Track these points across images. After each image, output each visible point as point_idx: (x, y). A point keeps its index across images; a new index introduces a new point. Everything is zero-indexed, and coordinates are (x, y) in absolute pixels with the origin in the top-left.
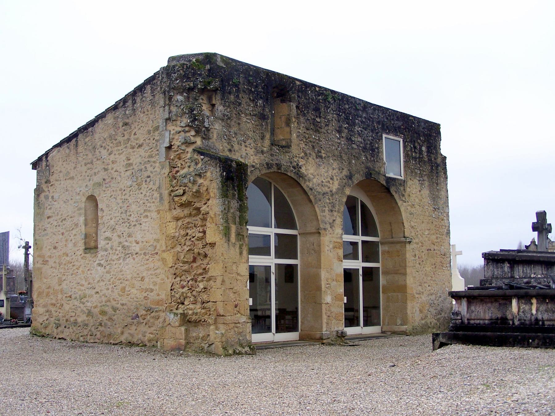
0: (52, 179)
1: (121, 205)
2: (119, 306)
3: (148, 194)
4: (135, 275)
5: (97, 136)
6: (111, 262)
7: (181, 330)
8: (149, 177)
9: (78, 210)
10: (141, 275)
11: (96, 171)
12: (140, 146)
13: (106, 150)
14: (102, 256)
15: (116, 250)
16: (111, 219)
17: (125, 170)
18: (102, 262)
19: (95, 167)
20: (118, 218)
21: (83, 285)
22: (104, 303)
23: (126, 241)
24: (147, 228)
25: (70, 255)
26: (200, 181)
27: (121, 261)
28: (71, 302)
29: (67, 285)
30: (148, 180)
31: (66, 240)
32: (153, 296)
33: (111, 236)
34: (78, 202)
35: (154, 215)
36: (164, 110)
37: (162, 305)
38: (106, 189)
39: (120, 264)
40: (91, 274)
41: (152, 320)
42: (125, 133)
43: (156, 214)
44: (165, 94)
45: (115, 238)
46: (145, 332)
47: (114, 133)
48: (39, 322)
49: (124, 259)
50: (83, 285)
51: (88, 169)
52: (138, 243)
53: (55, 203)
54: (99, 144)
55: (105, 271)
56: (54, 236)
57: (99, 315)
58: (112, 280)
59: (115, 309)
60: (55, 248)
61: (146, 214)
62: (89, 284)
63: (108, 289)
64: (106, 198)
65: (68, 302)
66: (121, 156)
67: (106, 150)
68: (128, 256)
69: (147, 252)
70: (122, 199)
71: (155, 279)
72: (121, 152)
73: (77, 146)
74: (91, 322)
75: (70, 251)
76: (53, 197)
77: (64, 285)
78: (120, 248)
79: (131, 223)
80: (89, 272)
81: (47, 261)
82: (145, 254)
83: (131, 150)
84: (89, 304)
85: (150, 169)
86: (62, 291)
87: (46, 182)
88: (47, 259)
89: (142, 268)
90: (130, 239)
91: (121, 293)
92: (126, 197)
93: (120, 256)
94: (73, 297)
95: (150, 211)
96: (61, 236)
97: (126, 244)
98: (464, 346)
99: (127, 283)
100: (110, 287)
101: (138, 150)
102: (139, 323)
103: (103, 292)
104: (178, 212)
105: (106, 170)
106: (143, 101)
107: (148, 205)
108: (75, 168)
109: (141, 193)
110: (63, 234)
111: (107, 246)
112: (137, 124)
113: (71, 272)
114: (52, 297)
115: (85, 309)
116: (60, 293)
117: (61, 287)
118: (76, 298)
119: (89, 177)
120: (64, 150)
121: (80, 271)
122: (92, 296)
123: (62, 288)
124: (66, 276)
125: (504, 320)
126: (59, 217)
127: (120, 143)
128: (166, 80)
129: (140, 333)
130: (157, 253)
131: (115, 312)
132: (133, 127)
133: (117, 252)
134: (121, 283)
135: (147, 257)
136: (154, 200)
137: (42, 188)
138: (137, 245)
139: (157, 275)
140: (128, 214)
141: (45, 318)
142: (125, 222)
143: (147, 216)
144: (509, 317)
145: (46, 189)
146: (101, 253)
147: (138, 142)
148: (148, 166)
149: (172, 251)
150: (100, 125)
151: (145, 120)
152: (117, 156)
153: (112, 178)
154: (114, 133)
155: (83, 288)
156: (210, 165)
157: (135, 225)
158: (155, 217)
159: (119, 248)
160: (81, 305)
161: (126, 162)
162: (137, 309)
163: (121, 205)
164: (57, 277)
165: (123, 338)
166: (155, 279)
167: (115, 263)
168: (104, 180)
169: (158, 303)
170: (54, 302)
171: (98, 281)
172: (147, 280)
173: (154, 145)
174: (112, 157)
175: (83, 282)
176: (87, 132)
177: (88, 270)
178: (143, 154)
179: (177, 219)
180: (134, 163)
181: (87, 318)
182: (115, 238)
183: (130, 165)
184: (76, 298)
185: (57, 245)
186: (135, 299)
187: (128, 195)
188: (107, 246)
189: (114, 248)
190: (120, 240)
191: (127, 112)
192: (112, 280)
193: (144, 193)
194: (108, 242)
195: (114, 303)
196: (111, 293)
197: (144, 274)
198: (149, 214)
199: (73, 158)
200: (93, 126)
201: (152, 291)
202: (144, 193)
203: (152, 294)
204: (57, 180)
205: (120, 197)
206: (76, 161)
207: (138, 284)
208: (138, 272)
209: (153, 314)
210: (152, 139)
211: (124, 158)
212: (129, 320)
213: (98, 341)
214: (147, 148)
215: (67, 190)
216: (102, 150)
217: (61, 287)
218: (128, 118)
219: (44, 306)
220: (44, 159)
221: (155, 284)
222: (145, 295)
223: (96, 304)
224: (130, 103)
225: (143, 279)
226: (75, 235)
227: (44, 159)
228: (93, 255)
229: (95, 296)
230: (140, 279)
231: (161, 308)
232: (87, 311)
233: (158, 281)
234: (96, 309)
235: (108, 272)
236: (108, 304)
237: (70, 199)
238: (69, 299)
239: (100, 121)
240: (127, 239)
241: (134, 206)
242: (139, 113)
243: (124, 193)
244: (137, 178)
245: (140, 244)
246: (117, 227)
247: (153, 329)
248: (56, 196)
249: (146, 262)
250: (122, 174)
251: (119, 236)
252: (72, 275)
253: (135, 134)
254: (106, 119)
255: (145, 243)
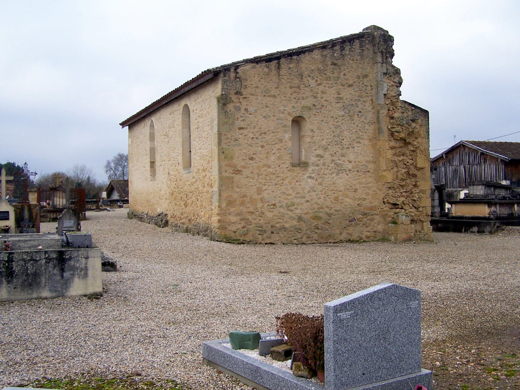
0: (244, 92)
1: (333, 129)
2: (332, 211)
3: (360, 125)
4: (348, 187)
5: (303, 66)
6: (323, 176)
7: (411, 226)
8: (360, 112)
9: (283, 126)
10: (354, 187)
11: (305, 96)
12: (350, 86)
13: (314, 81)
14: (313, 170)
15: (329, 166)
16: (323, 140)
17: (336, 101)
18: (313, 175)
19: (303, 92)
20: (330, 140)
21: (290, 195)
22: (316, 210)
23: (339, 160)
24: (360, 151)
25: (273, 167)
26: (414, 125)
27: (334, 175)
28: (276, 209)
29: (269, 194)
30: (360, 114)
31: (268, 153)
32: (366, 203)
33: (322, 154)
34: (282, 119)
35: (366, 142)
36: (382, 66)
37: (375, 210)
38: (317, 114)
39: (333, 178)
40: (300, 185)
41: (369, 222)
42: (335, 71)
43: (368, 141)
44: (382, 54)
45: (327, 155)
46: (363, 231)
47: (322, 68)
48: (231, 230)
49: (337, 174)
50: (290, 195)
51: (295, 92)
52: (350, 162)
53: (250, 116)
54: (306, 73)
55: (317, 183)
56: (250, 147)
57: (312, 220)
58: (324, 191)
59: (329, 215)
60: (252, 159)
61: (358, 140)
62: (298, 193)
63: (320, 198)
64: (316, 122)
65: (271, 210)
66: (331, 89)
67: (314, 81)
68: (341, 172)
69: (359, 170)
70: (334, 125)
71: (368, 191)
72: (330, 85)
73: (279, 68)
74: (304, 226)
75: (273, 163)
76: (246, 110)
77: (265, 195)
78: (333, 165)
79: (344, 145)
80: (297, 184)
81: (240, 171)
82: (358, 171)
83: (341, 87)
84: (298, 211)
85: (361, 106)
86: (262, 200)
87: (236, 93)
88: (239, 169)
89: (355, 182)
90: (343, 158)
91: (334, 201)
92: (338, 124)
93: (333, 170)
94: (278, 205)
95: (362, 139)
96: (260, 149)
97: (339, 162)
98: (441, 233)
99: (340, 193)
100: (322, 197)
101: (348, 88)
102: (357, 224)
103: (315, 201)
104: (393, 143)
105: (315, 97)
106: (352, 51)
107: (361, 134)
108: (277, 88)
109: (354, 123)
110: (262, 147)
111: (318, 162)
112: (346, 67)
113: (274, 182)
114: (248, 205)
115: (294, 215)
116: (260, 201)
117: (261, 196)
118: (281, 207)
119: (296, 100)
120: (262, 68)
121: (286, 182)
122: (302, 204)
123: (263, 197)
124: (267, 186)
125: (512, 214)
126: (257, 129)
127: (330, 78)
128: (383, 43)
129: (355, 232)
130: (369, 171)
131: (331, 217)
132: (342, 68)
133: (330, 168)
134: (334, 193)
135: (360, 174)
136: (366, 131)
137: (231, 98)
138: (350, 164)
139: (369, 188)
140: (341, 138)
141: (239, 226)
142: (337, 144)
143: (359, 142)
144: (514, 213)
145: (236, 101)
146: (310, 169)
147: (347, 82)
148: (359, 103)
149: (392, 171)
150: (306, 58)
151: (354, 66)
152: (327, 88)
153: (323, 106)
154: (322, 68)
155: (290, 197)
156: (421, 115)
157: (348, 148)
158: (366, 143)
159: (331, 165)
160: (289, 212)
161: (336, 96)
162: (353, 214)
163: (333, 129)
164: (255, 187)
165: (342, 238)
166: (368, 191)
167: (327, 176)
168: (314, 105)
169: (371, 208)
170: (251, 209)
171: (309, 192)
172: (359, 191)
173: (364, 89)
174: (321, 88)
175: (291, 192)
176: (291, 59)
177: (297, 181)
178: (353, 93)
179: (392, 148)
180: (345, 98)
181: (298, 224)
182: (327, 155)
183: (341, 98)
184: (281, 207)
185: (254, 156)
186: (349, 206)
187: (341, 122)
188: (318, 162)
189: (326, 164)
190: (332, 159)
191: (335, 55)
192: (324, 191)
193: (356, 124)
194: (319, 158)
195: (327, 210)
196: (323, 202)
197: (357, 187)
198: (361, 141)
199: (275, 78)
200: (298, 55)
201: (365, 199)
202: (356, 124)
203: (365, 202)
204: (252, 95)
205: (332, 123)
206: (277, 81)
207: (351, 194)
208: (351, 185)
209: (369, 217)
210: (361, 83)
211: (334, 92)
212: (347, 222)
213: (315, 241)
214: (357, 89)
215: (267, 106)
216: (310, 79)
217: (261, 196)
218: (337, 60)
219: (238, 214)
220: (232, 70)
221: (368, 194)
222: (359, 202)
223: (307, 211)
224: (337, 48)
225: (355, 191)
226: (279, 149)
227: (232, 70)
228: (302, 169)
229: (305, 204)
230: (353, 190)
231: (375, 212)
232: (297, 217)
233: (371, 192)
234: (307, 216)
235: (320, 184)
236: (321, 210)
237: (271, 115)
238: (272, 207)
239: (307, 54)
240: (340, 158)
241: (346, 133)
242: (348, 59)
243: (336, 120)
244: (349, 111)
245: (353, 163)
246: (329, 147)
247: (369, 228)
248: (251, 109)
249: (358, 178)
250: (333, 104)
251: (332, 155)
252: (276, 184)
253: (344, 75)
254: (313, 54)
255: (357, 163)
